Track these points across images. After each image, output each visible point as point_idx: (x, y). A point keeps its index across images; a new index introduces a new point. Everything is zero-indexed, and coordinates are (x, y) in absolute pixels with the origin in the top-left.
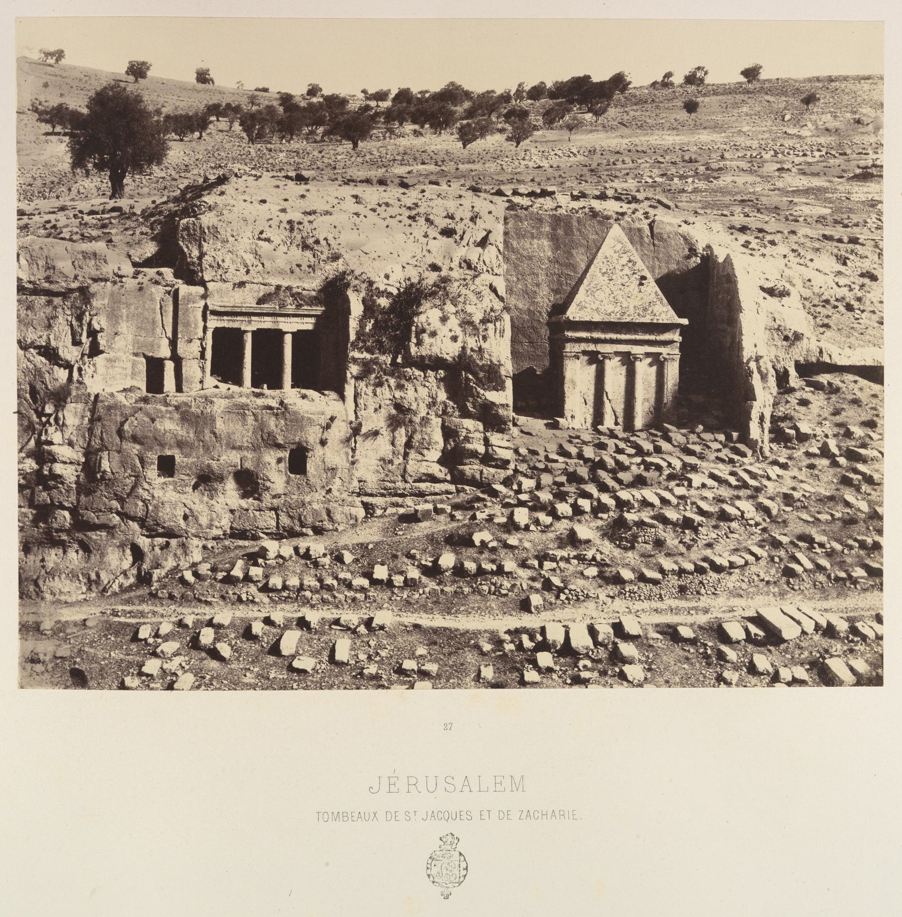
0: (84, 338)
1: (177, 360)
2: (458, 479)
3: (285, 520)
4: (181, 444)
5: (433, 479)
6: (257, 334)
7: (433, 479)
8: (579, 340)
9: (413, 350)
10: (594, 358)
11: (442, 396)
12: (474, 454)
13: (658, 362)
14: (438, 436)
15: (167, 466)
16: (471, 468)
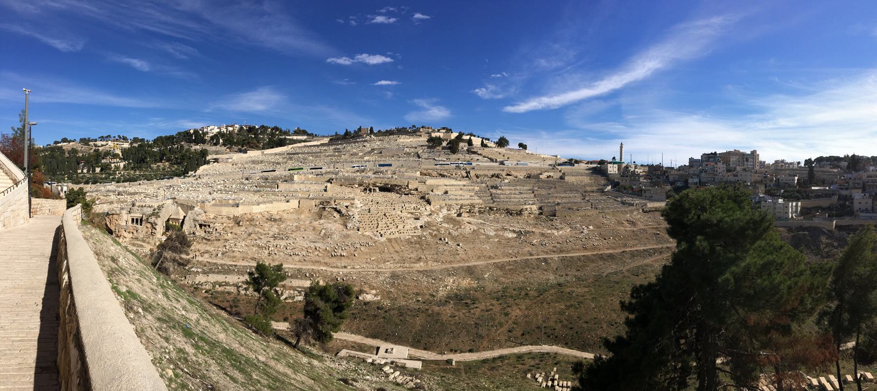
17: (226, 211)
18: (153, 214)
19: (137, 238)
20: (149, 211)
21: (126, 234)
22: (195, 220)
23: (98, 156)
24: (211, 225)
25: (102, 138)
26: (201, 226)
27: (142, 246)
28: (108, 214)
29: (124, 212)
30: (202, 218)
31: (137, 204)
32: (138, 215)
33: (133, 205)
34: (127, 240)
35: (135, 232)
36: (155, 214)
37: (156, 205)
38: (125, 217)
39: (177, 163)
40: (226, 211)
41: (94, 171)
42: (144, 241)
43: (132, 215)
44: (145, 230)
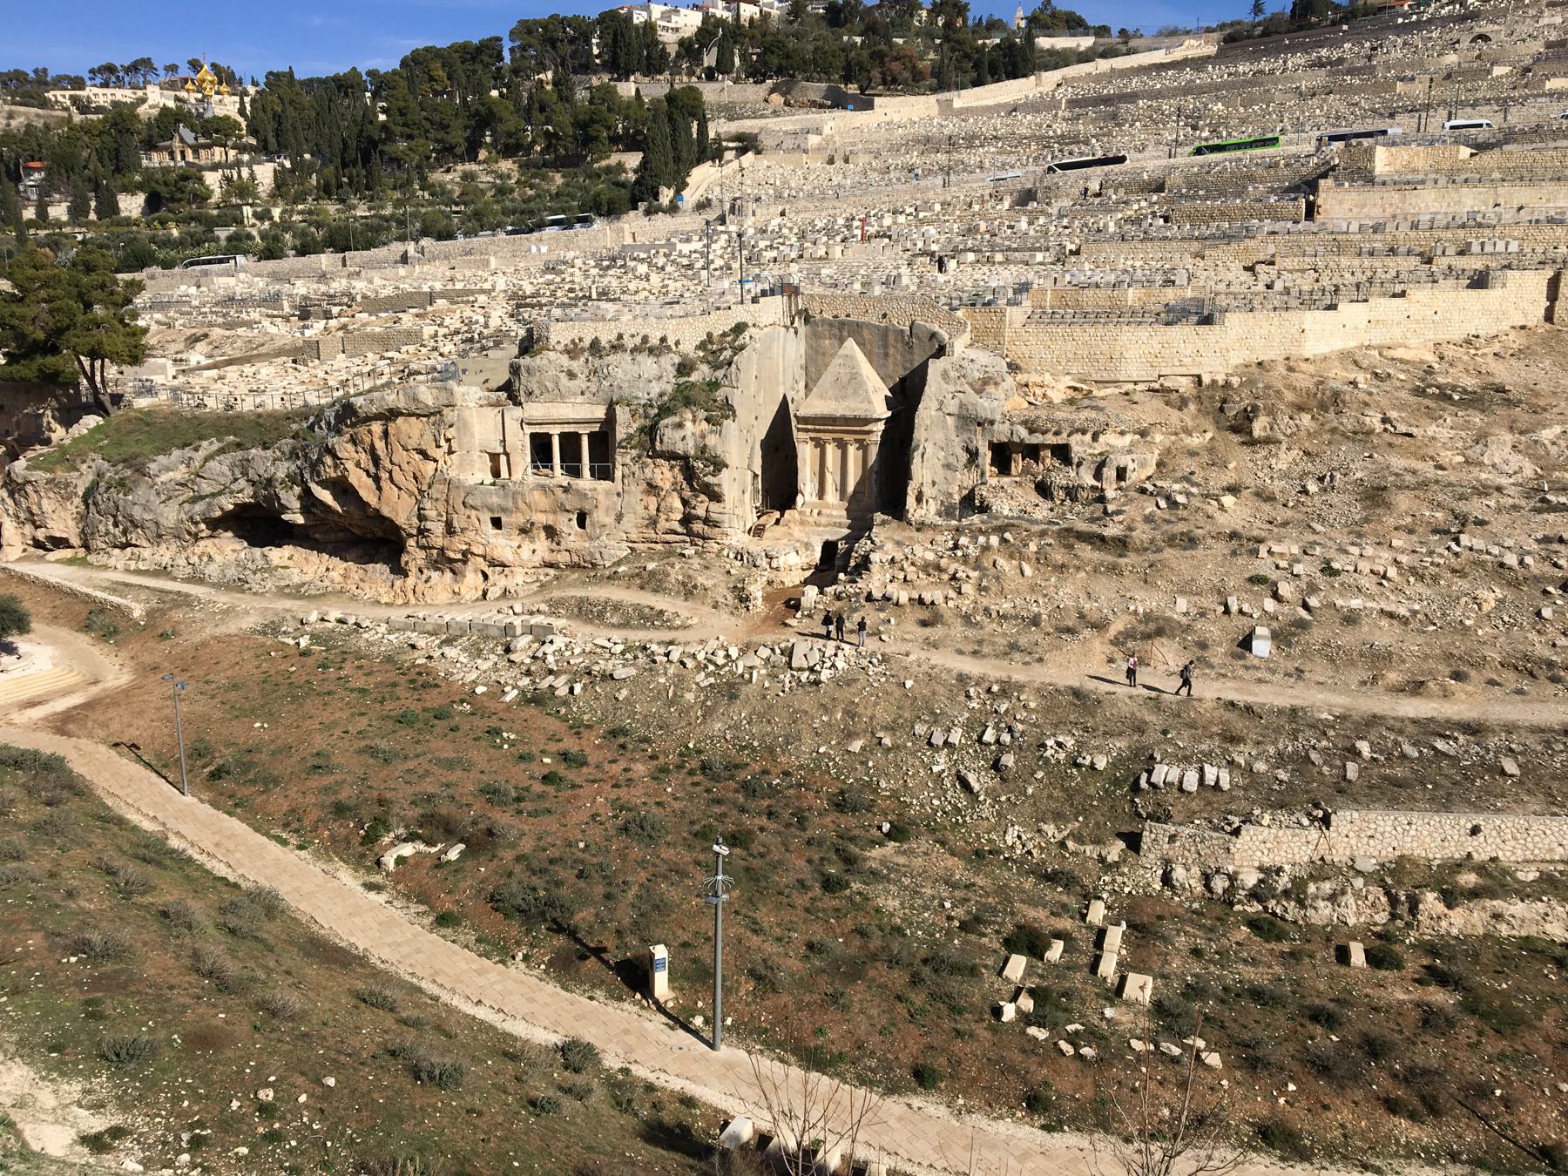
0: (442, 442)
1: (507, 455)
2: (690, 533)
3: (576, 559)
4: (504, 510)
5: (676, 533)
6: (562, 435)
7: (676, 533)
8: (807, 431)
9: (658, 446)
10: (820, 444)
11: (680, 477)
12: (698, 518)
13: (863, 447)
14: (678, 504)
15: (497, 523)
16: (698, 527)
17: (1145, 352)
18: (684, 398)
19: (585, 567)
20: (651, 379)
21: (503, 545)
22: (969, 420)
23: (121, 138)
24: (1080, 446)
25: (108, 74)
26: (1002, 455)
27: (652, 618)
28: (347, 415)
29: (469, 394)
30: (1005, 406)
31: (560, 334)
32: (576, 410)
33: (528, 346)
34: (518, 579)
35: (567, 524)
36: (701, 389)
37: (688, 336)
38: (482, 425)
39: (559, 164)
40: (1145, 352)
41: (109, 209)
42: (653, 582)
43: (534, 410)
44: (638, 505)
